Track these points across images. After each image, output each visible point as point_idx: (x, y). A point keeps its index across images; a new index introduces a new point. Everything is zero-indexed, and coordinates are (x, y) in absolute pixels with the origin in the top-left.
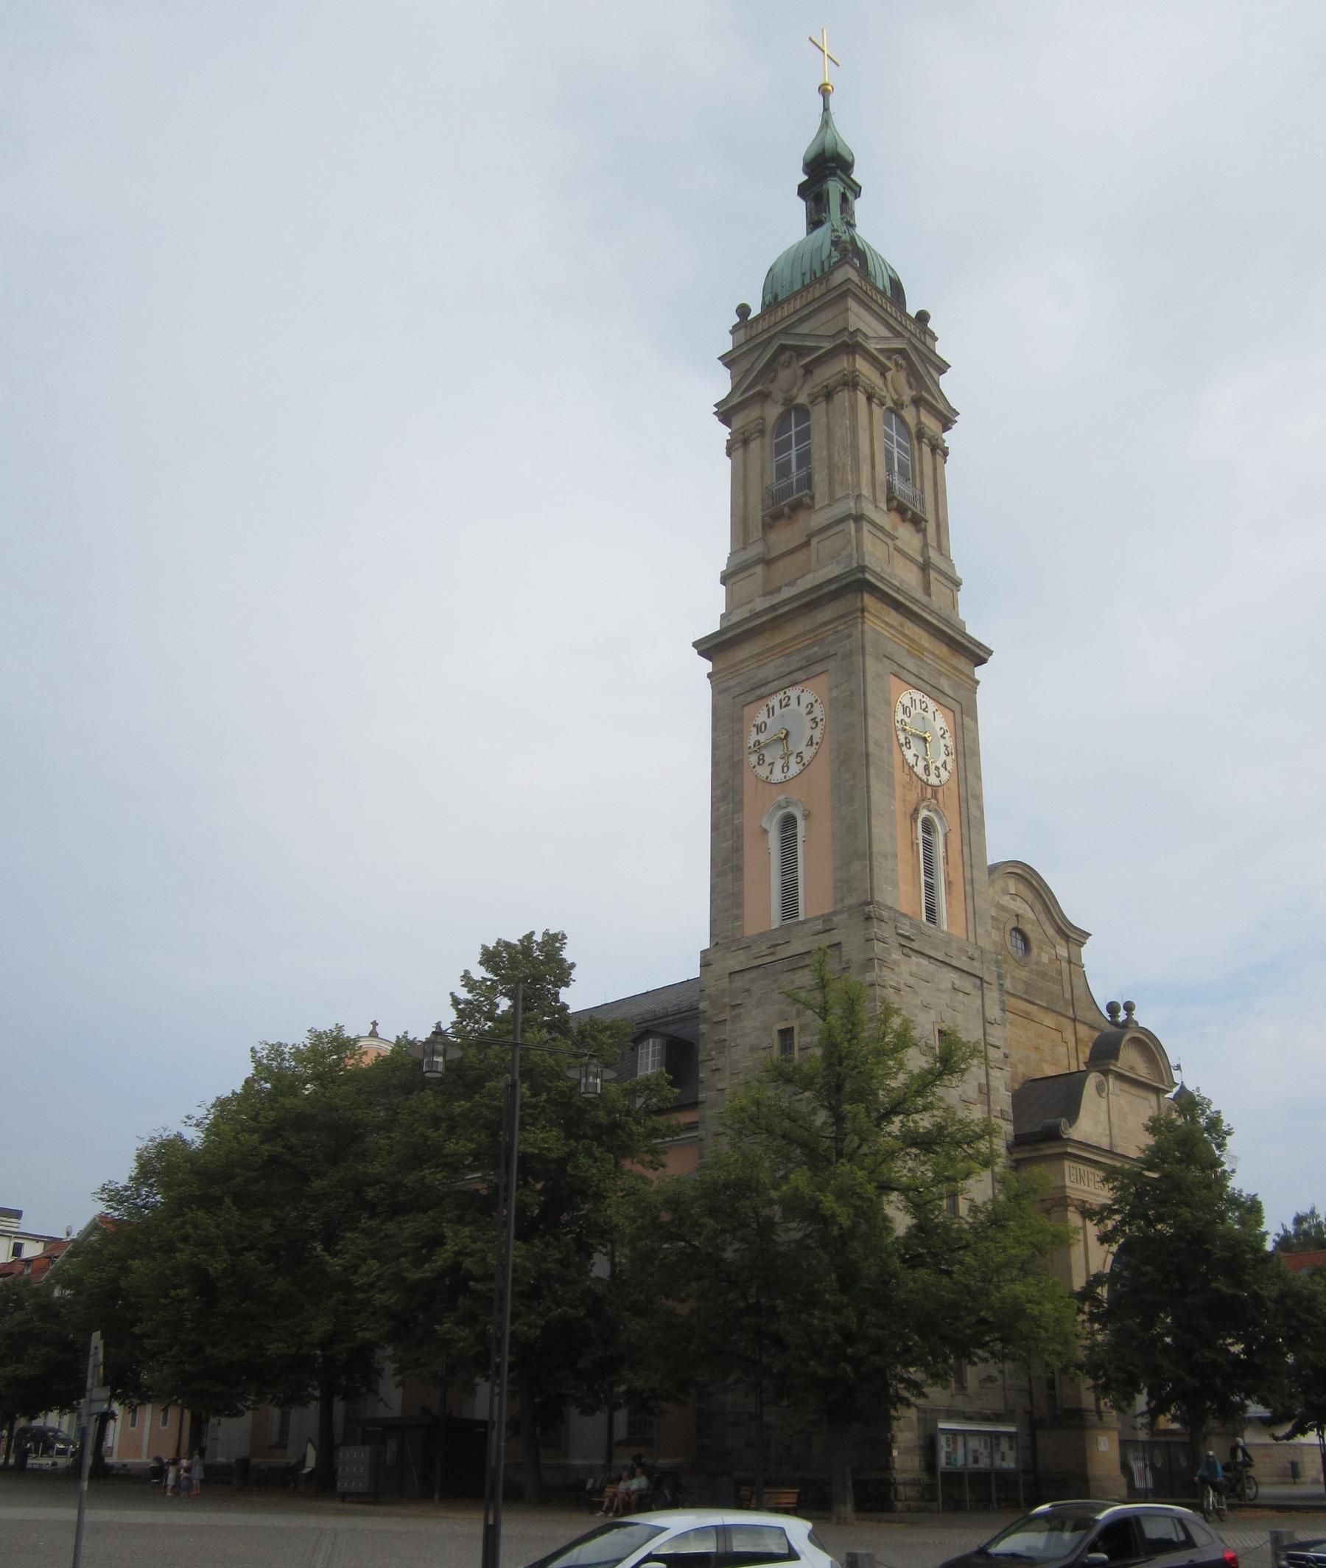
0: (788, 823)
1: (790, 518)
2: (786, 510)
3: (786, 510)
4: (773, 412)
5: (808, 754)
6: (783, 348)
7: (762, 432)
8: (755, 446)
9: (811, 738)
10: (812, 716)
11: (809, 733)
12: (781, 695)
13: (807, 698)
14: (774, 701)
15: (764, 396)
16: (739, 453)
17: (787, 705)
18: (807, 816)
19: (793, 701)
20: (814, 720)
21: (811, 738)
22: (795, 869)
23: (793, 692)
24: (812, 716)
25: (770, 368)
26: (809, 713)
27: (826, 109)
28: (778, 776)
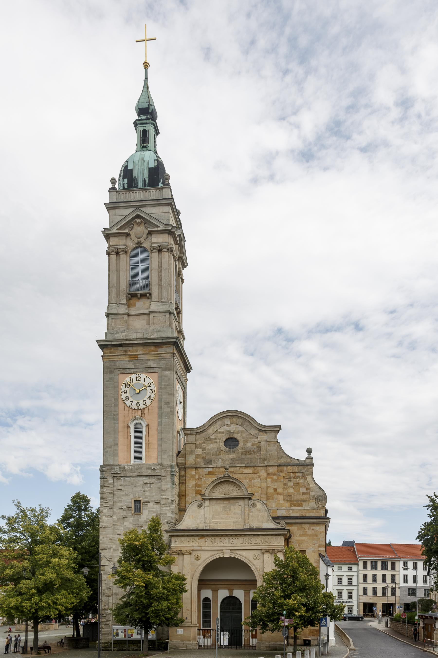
0: (138, 426)
1: (139, 299)
2: (139, 295)
3: (139, 295)
4: (131, 244)
5: (148, 402)
6: (138, 216)
7: (126, 252)
8: (122, 257)
9: (150, 397)
10: (151, 388)
11: (149, 394)
12: (136, 375)
13: (148, 380)
14: (134, 376)
15: (127, 235)
16: (114, 257)
17: (139, 380)
18: (148, 425)
19: (142, 380)
20: (151, 390)
21: (150, 397)
22: (141, 443)
23: (143, 376)
24: (151, 388)
25: (130, 223)
26: (149, 386)
27: (146, 78)
28: (134, 406)
